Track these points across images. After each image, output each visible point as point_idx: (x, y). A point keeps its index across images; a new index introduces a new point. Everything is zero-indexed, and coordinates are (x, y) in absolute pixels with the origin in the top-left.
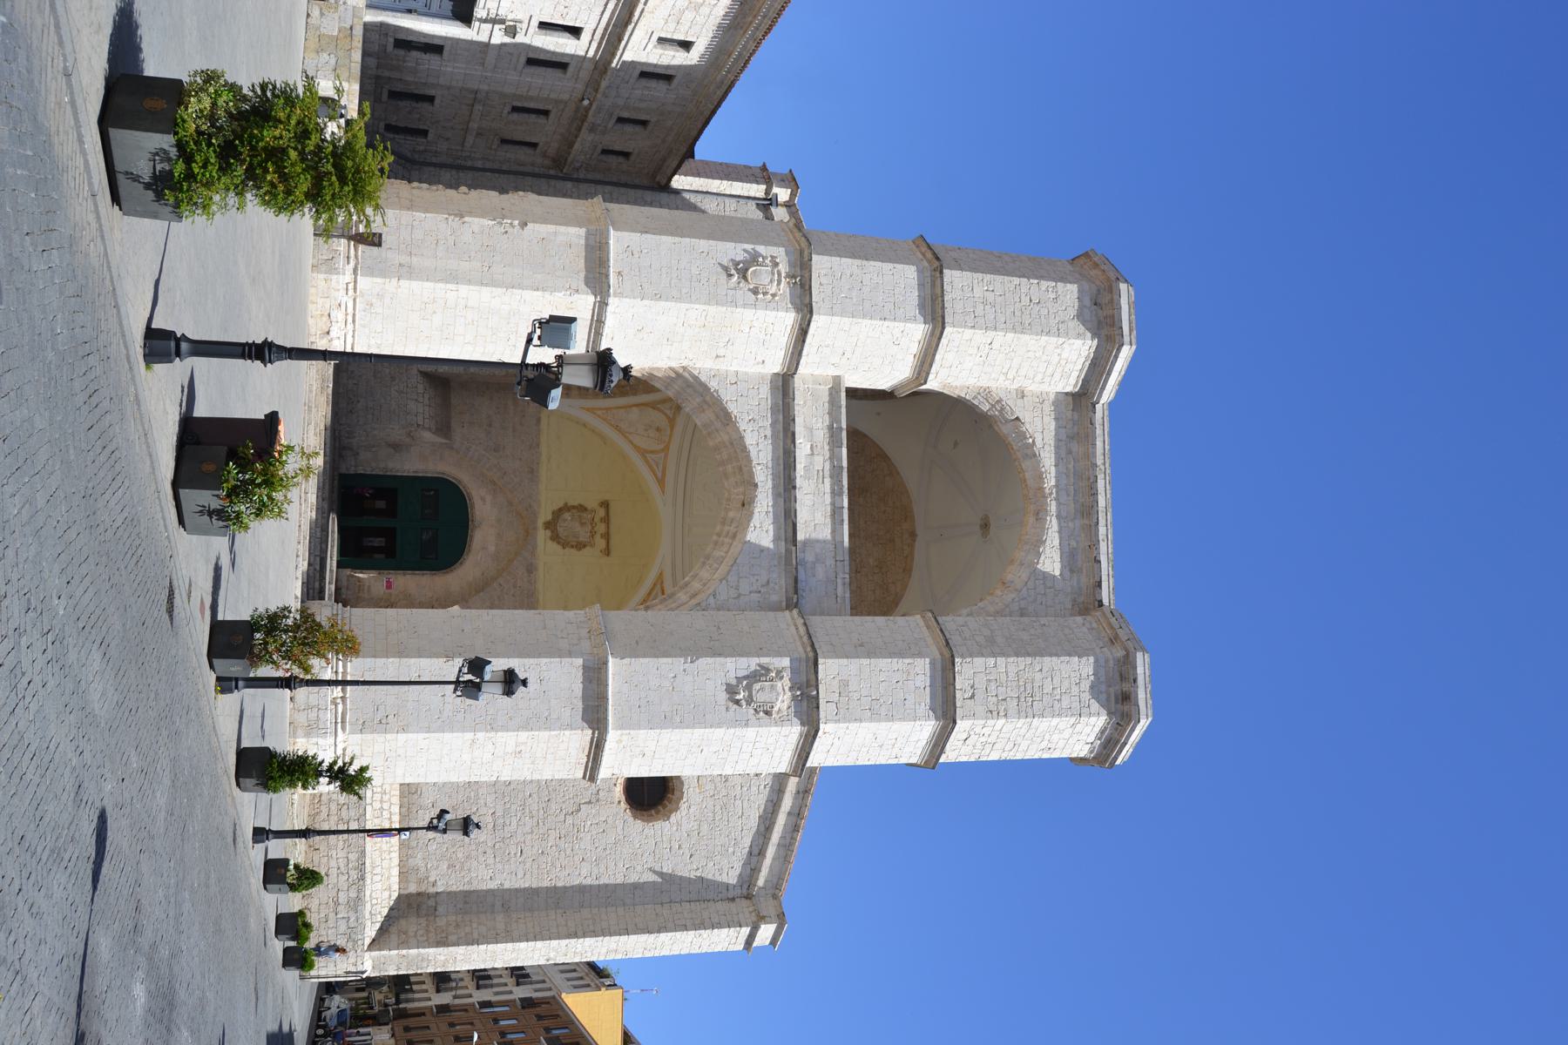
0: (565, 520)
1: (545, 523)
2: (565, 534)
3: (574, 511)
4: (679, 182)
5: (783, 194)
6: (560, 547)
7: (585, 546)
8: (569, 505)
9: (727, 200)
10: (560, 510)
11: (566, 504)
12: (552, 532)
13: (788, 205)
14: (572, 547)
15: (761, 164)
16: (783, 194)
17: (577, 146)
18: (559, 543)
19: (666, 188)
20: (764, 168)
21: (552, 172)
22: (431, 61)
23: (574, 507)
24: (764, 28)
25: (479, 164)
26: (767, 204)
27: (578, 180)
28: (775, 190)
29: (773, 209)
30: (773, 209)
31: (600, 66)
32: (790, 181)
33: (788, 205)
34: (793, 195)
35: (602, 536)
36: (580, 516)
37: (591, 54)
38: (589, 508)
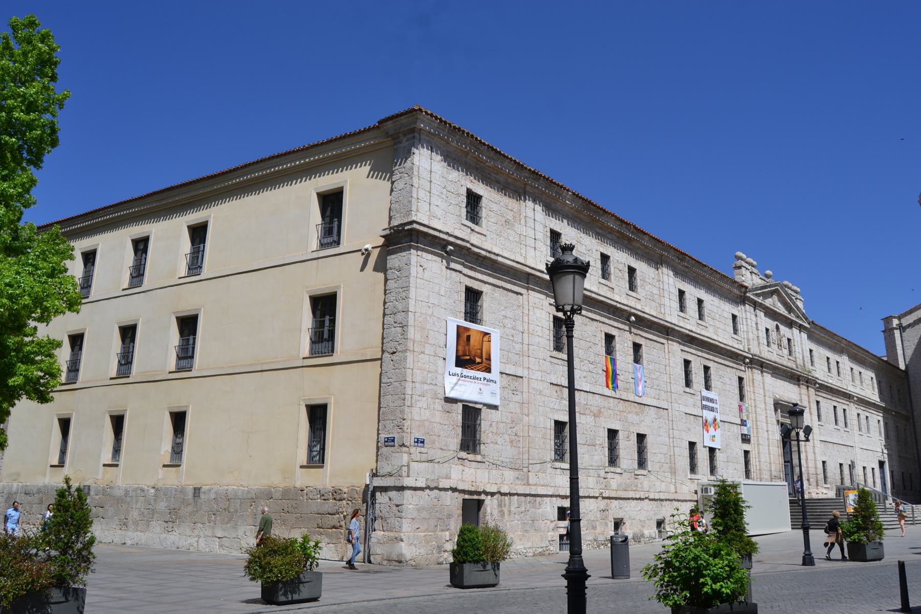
4: (902, 366)
5: (895, 322)
9: (905, 345)
13: (899, 318)
15: (882, 333)
16: (895, 322)
17: (904, 413)
19: (906, 372)
20: (884, 332)
21: (911, 421)
22: (895, 473)
24: (865, 353)
25: (916, 451)
26: (902, 328)
27: (912, 409)
28: (895, 326)
29: (904, 325)
30: (904, 325)
31: (885, 411)
32: (888, 320)
33: (899, 318)
34: (895, 317)
37: (881, 415)
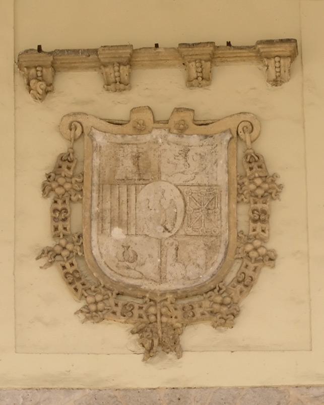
0: (129, 256)
1: (150, 353)
2: (200, 257)
3: (76, 212)
6: (267, 279)
7: (254, 160)
8: (48, 242)
10: (73, 279)
11: (50, 255)
12: (190, 316)
14: (260, 217)
18: (246, 283)
23: (60, 215)
35: (201, 80)
36: (109, 183)
38: (60, 146)
